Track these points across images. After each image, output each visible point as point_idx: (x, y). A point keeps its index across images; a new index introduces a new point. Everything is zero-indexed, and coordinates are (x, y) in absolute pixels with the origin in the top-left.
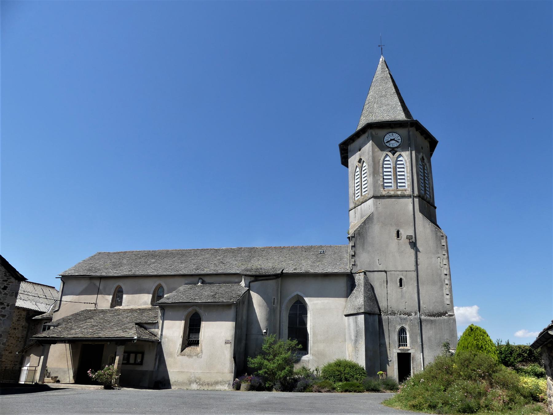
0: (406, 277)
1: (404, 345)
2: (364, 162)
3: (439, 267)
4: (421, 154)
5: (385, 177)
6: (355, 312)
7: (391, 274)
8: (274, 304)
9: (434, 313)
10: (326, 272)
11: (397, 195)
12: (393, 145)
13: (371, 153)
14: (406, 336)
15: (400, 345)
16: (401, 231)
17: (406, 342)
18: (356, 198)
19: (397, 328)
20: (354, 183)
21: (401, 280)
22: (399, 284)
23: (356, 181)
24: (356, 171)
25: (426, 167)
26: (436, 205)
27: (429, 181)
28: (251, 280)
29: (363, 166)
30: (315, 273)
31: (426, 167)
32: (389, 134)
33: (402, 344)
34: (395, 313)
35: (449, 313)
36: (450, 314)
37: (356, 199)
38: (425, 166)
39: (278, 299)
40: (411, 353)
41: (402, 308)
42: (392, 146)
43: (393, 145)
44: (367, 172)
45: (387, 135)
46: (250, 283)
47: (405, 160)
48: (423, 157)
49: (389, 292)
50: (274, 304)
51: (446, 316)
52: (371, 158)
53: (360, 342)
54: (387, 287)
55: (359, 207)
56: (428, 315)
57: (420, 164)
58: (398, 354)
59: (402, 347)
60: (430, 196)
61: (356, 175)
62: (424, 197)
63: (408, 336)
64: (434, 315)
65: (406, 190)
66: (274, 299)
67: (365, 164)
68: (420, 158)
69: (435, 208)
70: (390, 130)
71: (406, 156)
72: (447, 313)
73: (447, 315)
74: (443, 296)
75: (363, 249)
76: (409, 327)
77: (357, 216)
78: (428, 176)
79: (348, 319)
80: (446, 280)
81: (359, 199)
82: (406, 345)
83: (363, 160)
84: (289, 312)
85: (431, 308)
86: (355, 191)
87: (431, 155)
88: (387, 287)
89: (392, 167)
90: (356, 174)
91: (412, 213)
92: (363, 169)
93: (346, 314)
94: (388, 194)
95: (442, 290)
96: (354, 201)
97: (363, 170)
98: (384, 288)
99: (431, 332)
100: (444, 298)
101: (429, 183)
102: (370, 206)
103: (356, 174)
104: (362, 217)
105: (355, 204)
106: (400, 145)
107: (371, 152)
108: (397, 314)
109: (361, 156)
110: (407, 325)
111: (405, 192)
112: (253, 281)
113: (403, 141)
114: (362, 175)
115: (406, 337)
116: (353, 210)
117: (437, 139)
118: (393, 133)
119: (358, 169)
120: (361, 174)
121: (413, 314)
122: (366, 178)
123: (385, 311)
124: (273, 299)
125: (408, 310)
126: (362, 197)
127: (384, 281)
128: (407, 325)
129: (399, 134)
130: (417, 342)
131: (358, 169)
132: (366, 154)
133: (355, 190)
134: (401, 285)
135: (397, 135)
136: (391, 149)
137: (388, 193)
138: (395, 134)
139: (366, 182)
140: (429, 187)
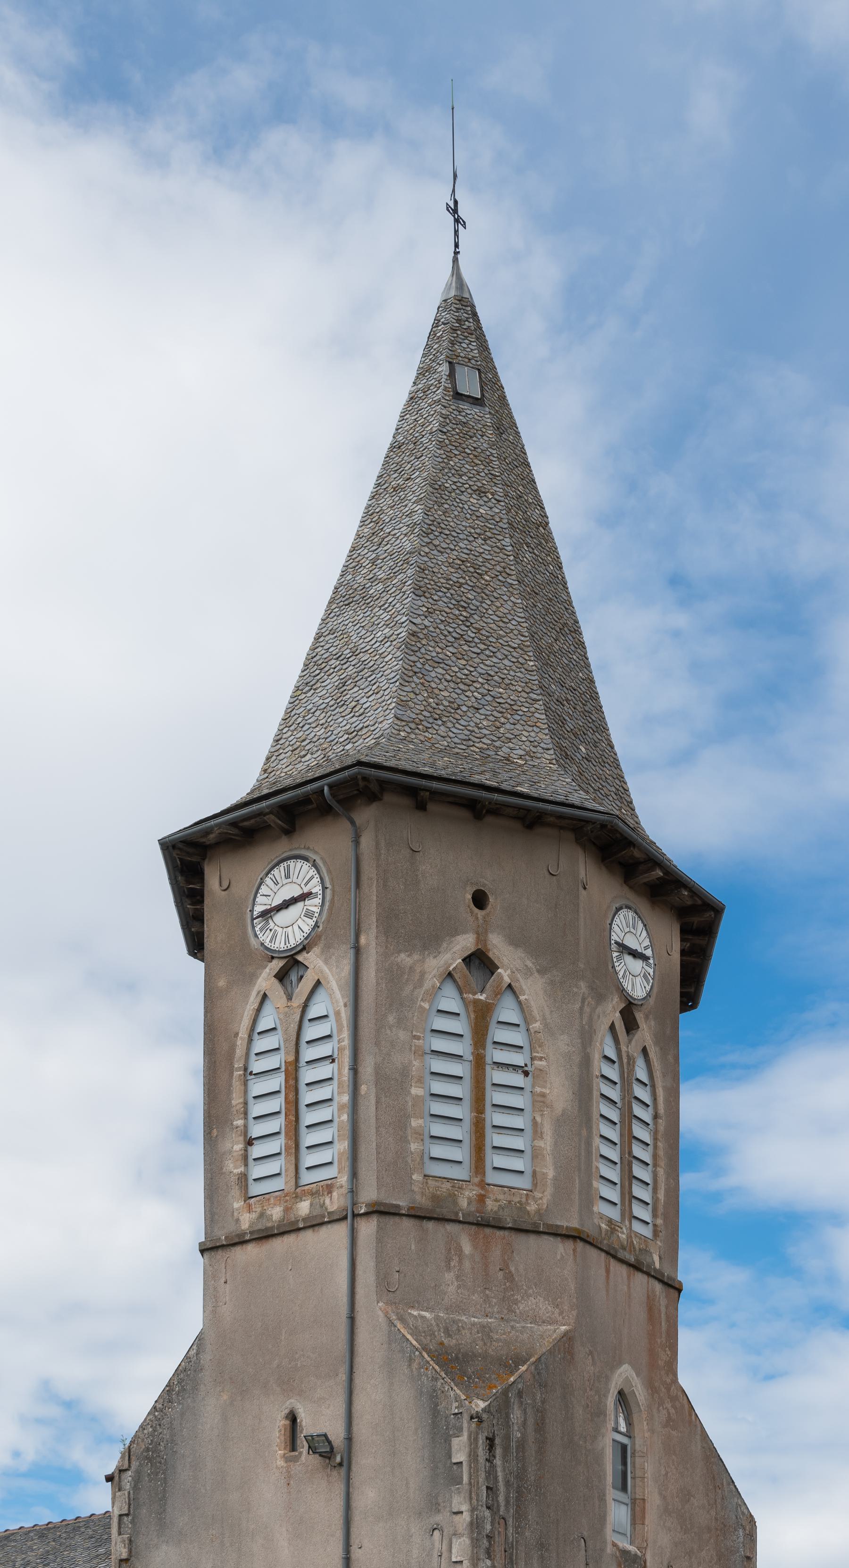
5: (257, 1130)
32: (276, 872)
42: (282, 947)
45: (268, 881)
65: (329, 1187)
70: (282, 847)
71: (341, 988)
91: (344, 1310)
94: (260, 1226)
106: (316, 925)
111: (327, 1201)
113: (332, 901)
118: (291, 863)
129: (315, 865)
135: (306, 866)
136: (277, 965)
137: (262, 1215)
138: (299, 863)
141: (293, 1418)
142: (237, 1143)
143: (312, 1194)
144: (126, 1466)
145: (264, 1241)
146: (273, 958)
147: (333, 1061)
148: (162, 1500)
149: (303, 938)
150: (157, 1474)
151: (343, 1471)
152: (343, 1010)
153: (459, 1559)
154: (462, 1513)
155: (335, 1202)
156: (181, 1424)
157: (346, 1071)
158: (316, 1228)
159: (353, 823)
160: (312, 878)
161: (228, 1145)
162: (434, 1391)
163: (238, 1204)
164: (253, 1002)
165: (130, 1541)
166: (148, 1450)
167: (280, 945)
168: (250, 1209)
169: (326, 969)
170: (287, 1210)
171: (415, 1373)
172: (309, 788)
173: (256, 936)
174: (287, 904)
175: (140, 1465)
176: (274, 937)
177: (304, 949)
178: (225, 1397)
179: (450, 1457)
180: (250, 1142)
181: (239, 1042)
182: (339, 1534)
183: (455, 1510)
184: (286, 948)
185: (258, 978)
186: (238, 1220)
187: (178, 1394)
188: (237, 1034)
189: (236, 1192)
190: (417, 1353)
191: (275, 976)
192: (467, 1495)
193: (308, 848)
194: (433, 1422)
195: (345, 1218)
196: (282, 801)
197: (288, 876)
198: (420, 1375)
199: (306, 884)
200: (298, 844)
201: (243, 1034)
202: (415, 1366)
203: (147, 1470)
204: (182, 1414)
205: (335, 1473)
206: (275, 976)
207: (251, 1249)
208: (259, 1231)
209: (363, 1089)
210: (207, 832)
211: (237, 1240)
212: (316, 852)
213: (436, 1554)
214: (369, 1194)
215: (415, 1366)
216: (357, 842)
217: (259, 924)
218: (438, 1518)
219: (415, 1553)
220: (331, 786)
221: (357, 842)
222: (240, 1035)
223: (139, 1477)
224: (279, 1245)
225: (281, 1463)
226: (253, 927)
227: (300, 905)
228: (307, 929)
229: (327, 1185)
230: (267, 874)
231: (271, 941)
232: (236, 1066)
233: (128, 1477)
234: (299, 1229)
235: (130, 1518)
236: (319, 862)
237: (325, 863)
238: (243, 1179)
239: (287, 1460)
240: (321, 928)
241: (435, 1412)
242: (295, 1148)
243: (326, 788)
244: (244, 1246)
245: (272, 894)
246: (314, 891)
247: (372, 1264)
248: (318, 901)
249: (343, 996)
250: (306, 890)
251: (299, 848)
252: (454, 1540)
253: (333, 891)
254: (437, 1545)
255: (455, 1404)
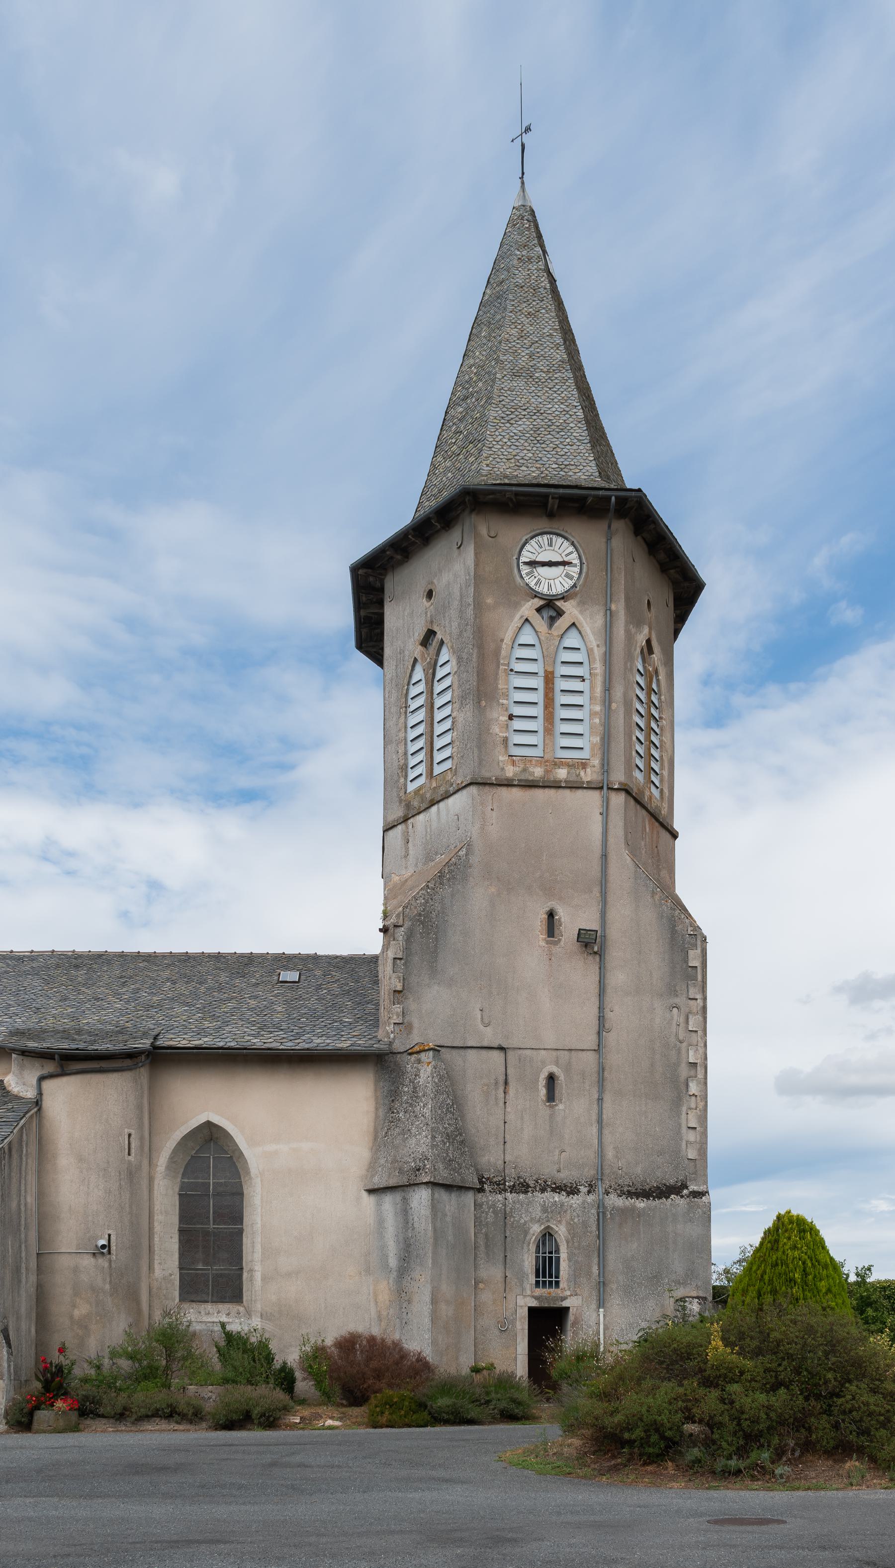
0: (568, 1069)
1: (551, 1282)
2: (442, 643)
3: (673, 1039)
4: (646, 630)
5: (518, 711)
6: (404, 1180)
7: (520, 1059)
8: (129, 1154)
9: (647, 1188)
10: (307, 1046)
11: (555, 781)
12: (550, 586)
13: (470, 612)
14: (559, 1257)
15: (537, 1283)
16: (562, 914)
17: (557, 1277)
18: (409, 783)
19: (531, 1231)
20: (406, 727)
21: (551, 1078)
22: (543, 1092)
23: (412, 720)
24: (413, 681)
25: (658, 680)
26: (677, 826)
27: (662, 736)
28: (45, 1072)
29: (440, 662)
30: (269, 1049)
31: (658, 680)
32: (539, 538)
33: (544, 1282)
34: (528, 1186)
35: (693, 1187)
36: (696, 1188)
37: (411, 787)
38: (654, 680)
39: (142, 1139)
40: (569, 1308)
41: (548, 1170)
42: (545, 591)
43: (550, 586)
44: (455, 686)
45: (533, 542)
46: (41, 1079)
47: (590, 653)
48: (649, 642)
49: (511, 1117)
50: (129, 1154)
51: (682, 1197)
52: (469, 634)
53: (416, 1274)
54: (505, 1103)
55: (421, 817)
56: (628, 1191)
57: (638, 670)
58: (531, 1310)
59: (544, 1290)
60: (662, 792)
61: (412, 695)
62: (643, 793)
63: (563, 1255)
64: (645, 1194)
65: (584, 765)
66: (130, 1135)
67: (444, 656)
68: (638, 645)
69: (674, 835)
70: (543, 523)
71: (594, 633)
72: (687, 1188)
73: (685, 1192)
74: (679, 1132)
75: (433, 971)
76: (569, 1231)
77: (411, 852)
78: (660, 718)
79: (379, 1205)
80: (691, 1084)
81: (421, 788)
82: (557, 1283)
83: (439, 636)
84: (179, 1179)
85: (639, 1170)
86: (406, 759)
87: (676, 633)
88: (505, 1103)
89: (542, 673)
90: (414, 691)
92: (440, 673)
93: (370, 1187)
94: (523, 777)
95: (679, 1114)
96: (402, 794)
97: (438, 677)
98: (497, 1104)
99: (635, 1245)
100: (681, 1139)
101: (661, 741)
102: (461, 818)
103: (414, 691)
104: (429, 858)
105: (408, 806)
106: (575, 586)
107: (472, 607)
108: (535, 1187)
109: (432, 622)
110: (564, 1222)
111: (582, 773)
112: (51, 1076)
113: (587, 573)
114: (435, 696)
115: (558, 1259)
116: (400, 827)
117: (704, 572)
118: (554, 537)
119: (419, 674)
120: (432, 693)
121: (583, 1190)
122: (447, 711)
123: (495, 1180)
124: (126, 1137)
125: (565, 1176)
126: (431, 783)
127: (496, 1083)
128: (564, 1222)
129: (573, 544)
130: (589, 1274)
131: (419, 674)
132: (453, 613)
133: (406, 754)
134: (551, 1096)
135: (566, 544)
136: (542, 603)
137: (525, 770)
138: (560, 540)
139: (447, 725)
140: (661, 757)
141: (551, 915)
142: (503, 715)
143: (569, 766)
144: (400, 923)
145: (527, 788)
146: (536, 596)
147: (584, 680)
148: (433, 955)
149: (563, 591)
150: (429, 934)
151: (597, 957)
152: (596, 649)
153: (694, 1029)
154: (697, 999)
155: (588, 776)
156: (451, 902)
157: (599, 689)
158: (574, 790)
159: (609, 527)
160: (571, 553)
161: (495, 715)
162: (673, 917)
163: (503, 758)
164: (517, 622)
165: (404, 978)
166: (420, 915)
167: (543, 589)
168: (514, 763)
169: (580, 617)
170: (547, 772)
171: (657, 902)
172: (601, 493)
173: (521, 577)
174: (550, 564)
175: (413, 925)
176: (538, 583)
177: (563, 598)
178: (493, 889)
179: (686, 961)
180: (511, 717)
181: (504, 646)
182: (595, 1001)
183: (691, 997)
184: (548, 593)
185: (521, 606)
186: (503, 769)
187: (449, 880)
188: (502, 640)
189: (500, 748)
190: (658, 889)
191: (535, 609)
192: (701, 988)
193: (566, 532)
194: (672, 937)
195: (601, 788)
196: (573, 494)
197: (550, 545)
198: (661, 905)
199: (567, 555)
200: (556, 525)
201: (508, 640)
202: (657, 897)
203: (420, 929)
204: (453, 895)
205: (590, 958)
206: (535, 609)
207: (516, 792)
208: (526, 780)
209: (614, 706)
210: (493, 492)
211: (506, 783)
212: (573, 537)
213: (674, 1023)
214: (618, 777)
215: (657, 897)
216: (609, 540)
217: (525, 570)
218: (677, 1000)
219: (658, 1020)
220: (616, 497)
221: (609, 540)
222: (505, 641)
223: (411, 933)
224: (539, 793)
225: (543, 944)
226: (519, 571)
227: (561, 568)
228: (567, 587)
229: (582, 763)
230: (532, 538)
231: (536, 584)
232: (502, 662)
233: (400, 932)
234: (560, 787)
235: (403, 961)
236: (576, 542)
237: (580, 546)
238: (505, 740)
239: (547, 942)
240: (578, 589)
241: (673, 931)
242: (549, 729)
243: (613, 499)
244: (510, 788)
245: (537, 554)
246: (574, 562)
247: (621, 824)
248: (577, 569)
249: (595, 639)
250: (566, 559)
251: (558, 529)
252: (690, 1016)
253: (588, 566)
254: (675, 1017)
255: (690, 929)
